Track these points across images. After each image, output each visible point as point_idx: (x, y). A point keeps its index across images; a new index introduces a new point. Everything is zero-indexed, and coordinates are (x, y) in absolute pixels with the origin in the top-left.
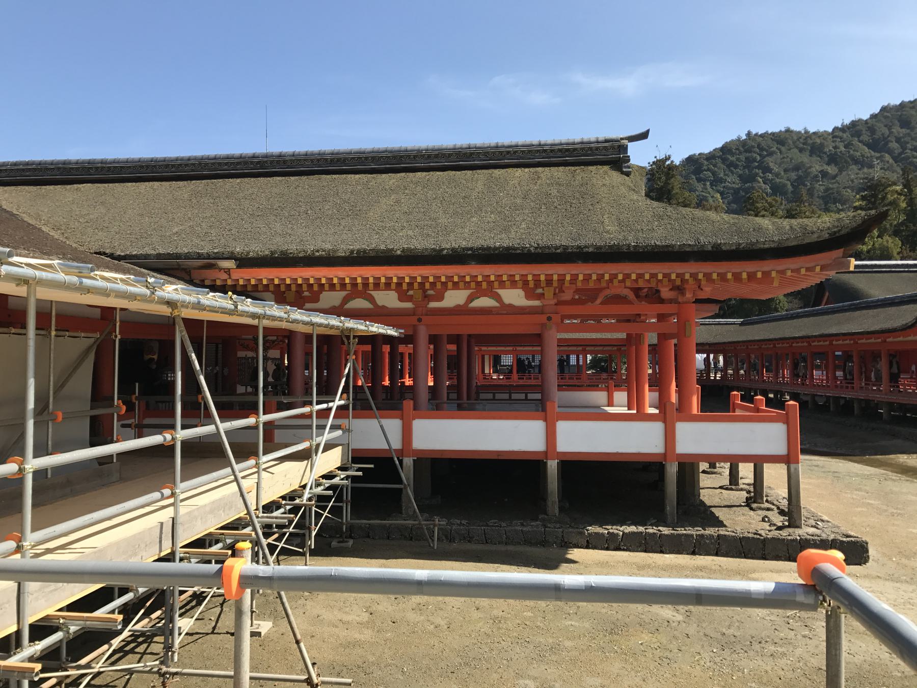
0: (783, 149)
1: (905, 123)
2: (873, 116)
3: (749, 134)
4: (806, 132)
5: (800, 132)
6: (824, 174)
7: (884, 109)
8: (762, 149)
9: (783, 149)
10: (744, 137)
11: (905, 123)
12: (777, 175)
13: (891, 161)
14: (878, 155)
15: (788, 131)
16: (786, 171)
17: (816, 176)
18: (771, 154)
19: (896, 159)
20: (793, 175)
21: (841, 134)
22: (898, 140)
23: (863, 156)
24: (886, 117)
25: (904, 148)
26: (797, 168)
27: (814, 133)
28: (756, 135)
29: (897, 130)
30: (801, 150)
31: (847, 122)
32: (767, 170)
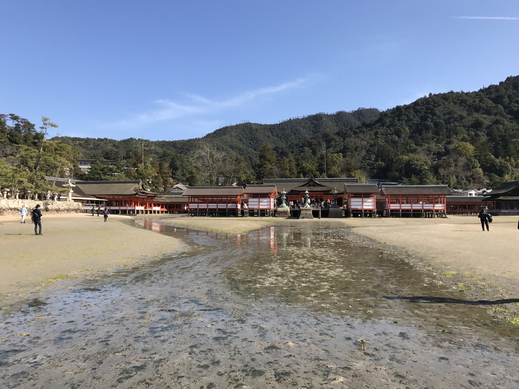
2: (501, 83)
3: (430, 94)
4: (463, 93)
5: (459, 93)
6: (461, 118)
7: (508, 79)
8: (435, 103)
9: (446, 103)
10: (428, 96)
12: (439, 117)
13: (502, 108)
14: (494, 105)
15: (452, 92)
16: (444, 115)
18: (439, 106)
19: (505, 108)
20: (447, 116)
21: (481, 93)
22: (509, 97)
23: (487, 106)
24: (506, 84)
25: (511, 101)
26: (449, 113)
28: (434, 95)
29: (511, 92)
30: (455, 103)
31: (487, 86)
32: (434, 114)
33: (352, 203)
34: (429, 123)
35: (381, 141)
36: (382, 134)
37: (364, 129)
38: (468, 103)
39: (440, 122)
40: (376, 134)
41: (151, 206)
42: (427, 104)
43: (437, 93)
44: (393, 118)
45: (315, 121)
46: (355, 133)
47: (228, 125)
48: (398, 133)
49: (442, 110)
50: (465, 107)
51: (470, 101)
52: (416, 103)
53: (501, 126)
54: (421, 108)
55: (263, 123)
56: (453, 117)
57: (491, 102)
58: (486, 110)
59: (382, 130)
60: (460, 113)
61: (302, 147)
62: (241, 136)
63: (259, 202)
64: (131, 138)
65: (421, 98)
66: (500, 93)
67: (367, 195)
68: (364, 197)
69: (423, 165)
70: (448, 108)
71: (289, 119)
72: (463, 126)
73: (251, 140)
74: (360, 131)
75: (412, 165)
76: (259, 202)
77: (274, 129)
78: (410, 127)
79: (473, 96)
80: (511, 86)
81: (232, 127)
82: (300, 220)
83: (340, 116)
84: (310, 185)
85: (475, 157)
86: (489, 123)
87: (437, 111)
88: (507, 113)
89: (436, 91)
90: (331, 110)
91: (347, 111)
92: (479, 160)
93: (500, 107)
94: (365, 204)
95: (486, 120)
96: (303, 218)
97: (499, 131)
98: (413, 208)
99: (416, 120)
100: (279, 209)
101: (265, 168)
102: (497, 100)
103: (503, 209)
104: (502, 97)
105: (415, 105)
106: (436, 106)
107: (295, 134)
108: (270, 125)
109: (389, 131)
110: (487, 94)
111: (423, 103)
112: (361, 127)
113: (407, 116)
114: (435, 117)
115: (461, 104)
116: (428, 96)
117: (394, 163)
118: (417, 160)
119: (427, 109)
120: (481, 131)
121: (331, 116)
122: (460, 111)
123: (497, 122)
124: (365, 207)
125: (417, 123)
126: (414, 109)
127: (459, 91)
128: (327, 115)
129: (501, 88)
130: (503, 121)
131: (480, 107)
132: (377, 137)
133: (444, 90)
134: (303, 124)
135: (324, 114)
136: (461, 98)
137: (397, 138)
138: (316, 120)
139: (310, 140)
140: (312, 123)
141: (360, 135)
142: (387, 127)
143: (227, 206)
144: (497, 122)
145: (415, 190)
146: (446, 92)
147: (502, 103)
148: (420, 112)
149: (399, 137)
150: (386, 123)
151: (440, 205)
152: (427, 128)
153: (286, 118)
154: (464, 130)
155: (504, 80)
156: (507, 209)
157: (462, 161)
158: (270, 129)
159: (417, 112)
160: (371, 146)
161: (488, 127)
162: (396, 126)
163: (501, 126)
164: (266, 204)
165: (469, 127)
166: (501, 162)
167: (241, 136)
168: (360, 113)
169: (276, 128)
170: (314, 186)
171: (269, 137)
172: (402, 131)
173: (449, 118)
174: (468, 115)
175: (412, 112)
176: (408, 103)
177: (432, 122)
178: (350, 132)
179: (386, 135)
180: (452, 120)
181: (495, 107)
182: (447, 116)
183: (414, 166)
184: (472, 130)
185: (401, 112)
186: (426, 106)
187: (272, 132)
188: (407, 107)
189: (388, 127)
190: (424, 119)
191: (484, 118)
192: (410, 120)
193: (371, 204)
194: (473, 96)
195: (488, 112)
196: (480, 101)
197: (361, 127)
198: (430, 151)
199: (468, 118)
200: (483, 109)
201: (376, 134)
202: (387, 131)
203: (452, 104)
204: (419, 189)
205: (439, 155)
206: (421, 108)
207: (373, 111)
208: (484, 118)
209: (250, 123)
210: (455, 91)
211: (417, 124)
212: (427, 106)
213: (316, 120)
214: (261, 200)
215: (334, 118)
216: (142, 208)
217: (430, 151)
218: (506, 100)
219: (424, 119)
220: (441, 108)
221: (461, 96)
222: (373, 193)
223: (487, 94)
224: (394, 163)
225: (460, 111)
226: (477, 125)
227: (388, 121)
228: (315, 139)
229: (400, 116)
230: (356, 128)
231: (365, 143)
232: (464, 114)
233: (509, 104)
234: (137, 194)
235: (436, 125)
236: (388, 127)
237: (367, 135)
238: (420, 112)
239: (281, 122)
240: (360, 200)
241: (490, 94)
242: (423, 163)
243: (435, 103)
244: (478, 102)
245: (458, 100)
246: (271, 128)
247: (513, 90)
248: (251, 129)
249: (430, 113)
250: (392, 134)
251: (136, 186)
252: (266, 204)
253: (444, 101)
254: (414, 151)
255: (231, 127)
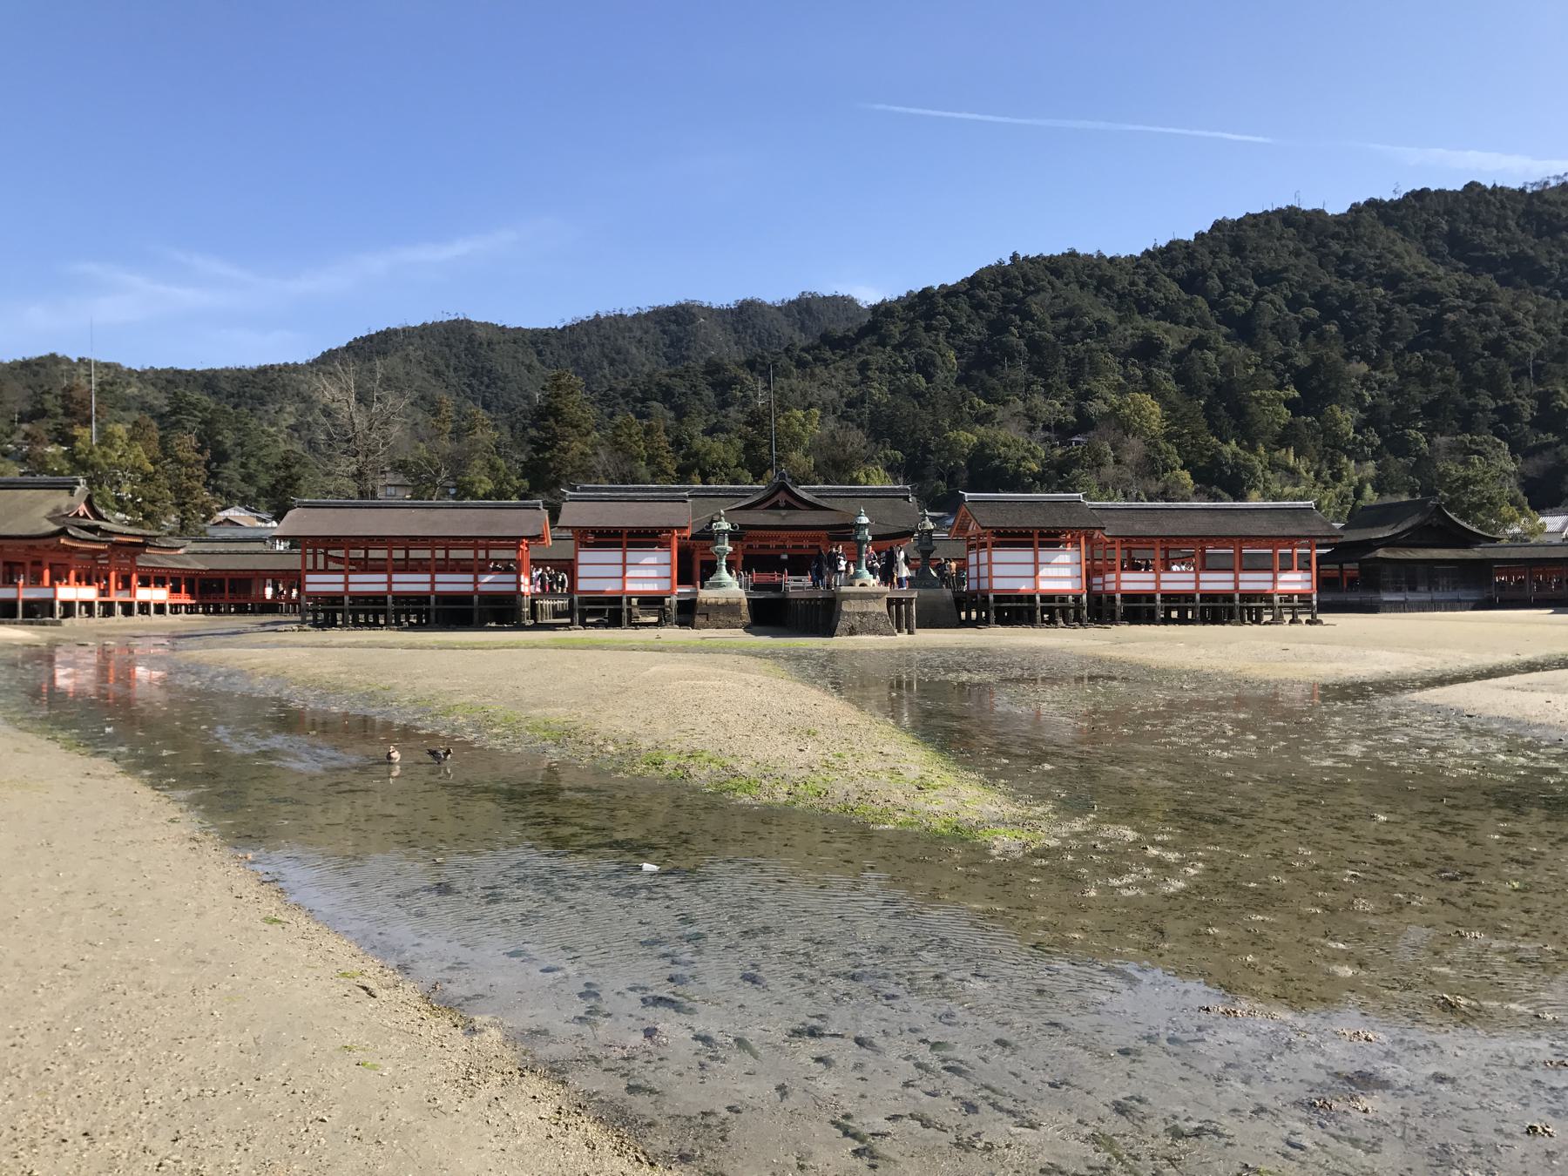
0: (1058, 283)
1: (1238, 248)
3: (1014, 257)
4: (1101, 257)
6: (1103, 328)
7: (1217, 225)
8: (1027, 282)
9: (1058, 283)
11: (1238, 248)
12: (1041, 324)
13: (1205, 307)
14: (1185, 297)
15: (1073, 254)
16: (1054, 317)
17: (1090, 328)
18: (1038, 291)
19: (1213, 305)
20: (1063, 322)
22: (1222, 276)
23: (1166, 299)
24: (1213, 238)
25: (1227, 288)
26: (1069, 314)
27: (1112, 260)
28: (1026, 258)
29: (1226, 261)
30: (1083, 286)
31: (1163, 243)
32: (1027, 315)
33: (997, 570)
34: (1014, 339)
35: (879, 391)
36: (881, 370)
37: (828, 354)
38: (1118, 287)
39: (1045, 340)
40: (863, 367)
41: (127, 585)
42: (1007, 284)
43: (1033, 255)
44: (912, 321)
45: (673, 327)
46: (801, 364)
47: (395, 324)
48: (925, 367)
49: (1047, 302)
50: (1108, 297)
51: (1122, 283)
52: (974, 281)
53: (1210, 356)
54: (990, 297)
55: (512, 323)
56: (1079, 325)
57: (1175, 287)
58: (1163, 309)
59: (879, 357)
60: (1097, 315)
61: (643, 400)
62: (437, 360)
63: (624, 564)
64: (53, 356)
65: (990, 267)
66: (1198, 264)
67: (1050, 539)
68: (1042, 545)
69: (1024, 458)
70: (1066, 300)
71: (592, 315)
72: (1111, 351)
73: (473, 375)
74: (816, 359)
75: (992, 458)
76: (624, 564)
77: (547, 343)
78: (960, 350)
79: (1129, 266)
80: (1226, 247)
81: (408, 332)
82: (839, 642)
83: (746, 315)
84: (775, 506)
85: (1168, 437)
86: (1178, 346)
87: (1035, 305)
88: (1218, 322)
89: (1032, 248)
90: (721, 293)
91: (769, 301)
92: (1178, 446)
93: (1200, 301)
94: (1043, 572)
95: (1172, 338)
96: (852, 631)
97: (1207, 370)
98: (1204, 587)
99: (977, 331)
100: (706, 595)
101: (565, 450)
102: (1192, 283)
103: (1386, 589)
104: (1204, 275)
105: (972, 288)
106: (1032, 293)
107: (612, 363)
108: (534, 332)
109: (900, 361)
110: (1164, 265)
111: (994, 281)
112: (818, 347)
113: (952, 318)
114: (1029, 325)
115: (1098, 289)
116: (1008, 262)
117: (931, 452)
118: (1004, 445)
119: (1008, 298)
120: (1159, 367)
121: (721, 313)
122: (1098, 310)
123: (1200, 344)
124: (1045, 586)
125: (978, 338)
126: (971, 297)
127: (1092, 251)
128: (709, 309)
129: (1200, 249)
130: (1216, 341)
131: (1150, 300)
132: (866, 379)
133: (1054, 247)
134: (638, 334)
135: (701, 307)
136: (1097, 272)
137: (923, 380)
138: (676, 322)
139: (665, 381)
140: (664, 332)
141: (817, 371)
142: (894, 348)
143: (476, 582)
144: (1200, 344)
145: (1206, 519)
146: (1057, 252)
147: (1204, 293)
148: (987, 308)
149: (929, 378)
150: (891, 336)
151: (1296, 576)
152: (1011, 354)
153: (585, 312)
154: (1112, 361)
155: (1206, 228)
156: (1399, 590)
157: (1135, 448)
158: (534, 344)
159: (978, 306)
160: (850, 404)
161: (1179, 357)
162: (920, 345)
163: (1210, 356)
164: (653, 573)
165: (1127, 355)
166: (1235, 455)
167: (437, 360)
168: (804, 309)
169: (553, 341)
170: (789, 506)
171: (529, 368)
172: (939, 360)
173: (1069, 329)
174: (1121, 320)
175: (966, 307)
176: (951, 281)
177: (1021, 337)
178: (784, 361)
179: (892, 372)
180: (1076, 334)
181: (1189, 303)
182: (1063, 322)
183: (997, 462)
184: (1134, 364)
185: (933, 305)
186: (1003, 289)
187: (539, 353)
188: (949, 293)
189: (898, 348)
190: (998, 327)
191: (1167, 331)
192: (960, 330)
193: (1066, 572)
194: (1129, 266)
195: (1169, 314)
196: (1148, 284)
197: (818, 347)
198: (1033, 419)
199: (1120, 328)
200: (1156, 306)
201: (863, 367)
202: (895, 362)
203: (1075, 286)
204: (1221, 518)
205: (1062, 432)
206: (990, 297)
207: (843, 304)
208: (1167, 331)
209: (469, 322)
210: (1081, 251)
211: (978, 343)
212: (1007, 291)
213: (676, 322)
214: (632, 556)
215: (729, 318)
216: (89, 593)
217: (1033, 419)
218: (1215, 283)
219: (998, 327)
220: (1046, 296)
221: (1098, 266)
222: (1064, 530)
223: (1164, 265)
224: (931, 452)
225: (1098, 310)
226: (1148, 350)
227: (896, 330)
228: (682, 377)
229: (933, 317)
230: (803, 350)
231: (834, 393)
232: (1111, 317)
233: (1222, 295)
234: (63, 532)
235: (1034, 346)
236: (898, 348)
237: (836, 370)
238: (987, 308)
239: (568, 322)
240: (1026, 555)
241: (1174, 265)
242: (1022, 453)
243: (1027, 282)
244: (1142, 286)
245: (1089, 276)
246: (539, 340)
247: (1232, 256)
248: (471, 340)
249: (1015, 311)
250: (910, 371)
251: (61, 499)
252: (653, 573)
253: (1053, 278)
254: (984, 419)
255: (404, 330)
